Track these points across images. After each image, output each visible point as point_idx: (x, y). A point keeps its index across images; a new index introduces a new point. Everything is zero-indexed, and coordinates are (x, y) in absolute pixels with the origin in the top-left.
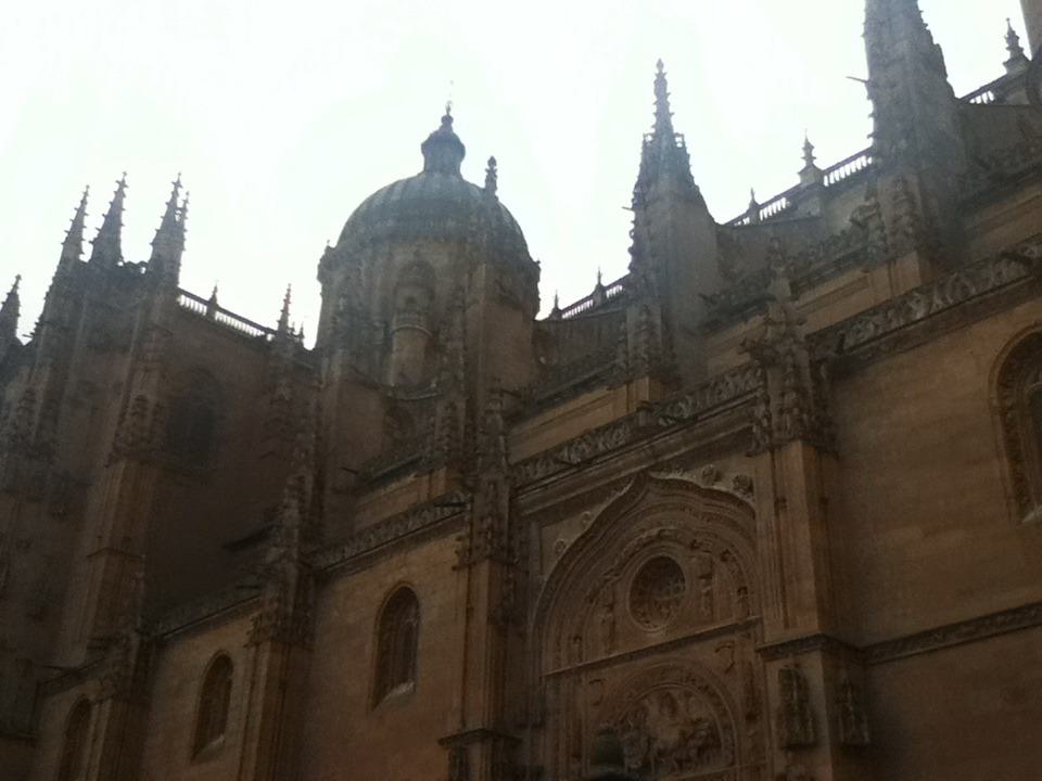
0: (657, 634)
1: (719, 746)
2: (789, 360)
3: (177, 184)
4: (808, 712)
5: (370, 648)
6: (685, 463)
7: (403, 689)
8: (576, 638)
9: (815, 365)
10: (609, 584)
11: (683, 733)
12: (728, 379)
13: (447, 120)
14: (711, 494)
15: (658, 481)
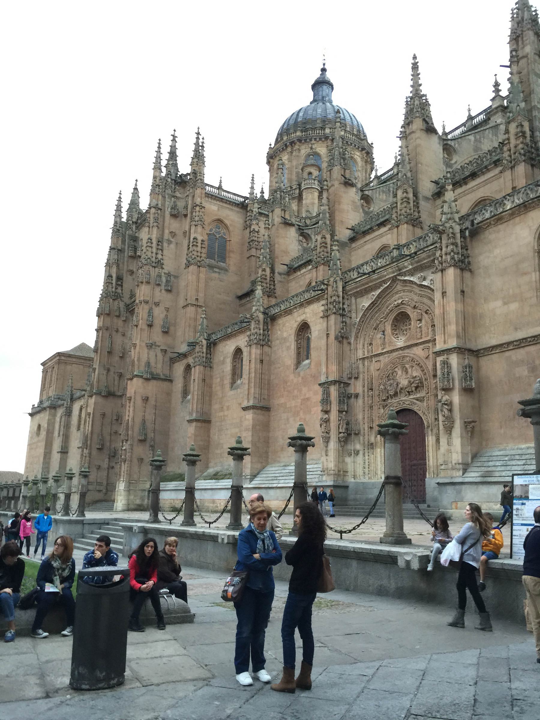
0: (400, 343)
1: (423, 387)
2: (451, 230)
3: (198, 134)
4: (451, 377)
5: (293, 346)
6: (412, 273)
7: (307, 362)
8: (370, 344)
9: (462, 231)
10: (383, 322)
11: (410, 382)
12: (430, 235)
13: (324, 70)
14: (421, 286)
15: (401, 280)
